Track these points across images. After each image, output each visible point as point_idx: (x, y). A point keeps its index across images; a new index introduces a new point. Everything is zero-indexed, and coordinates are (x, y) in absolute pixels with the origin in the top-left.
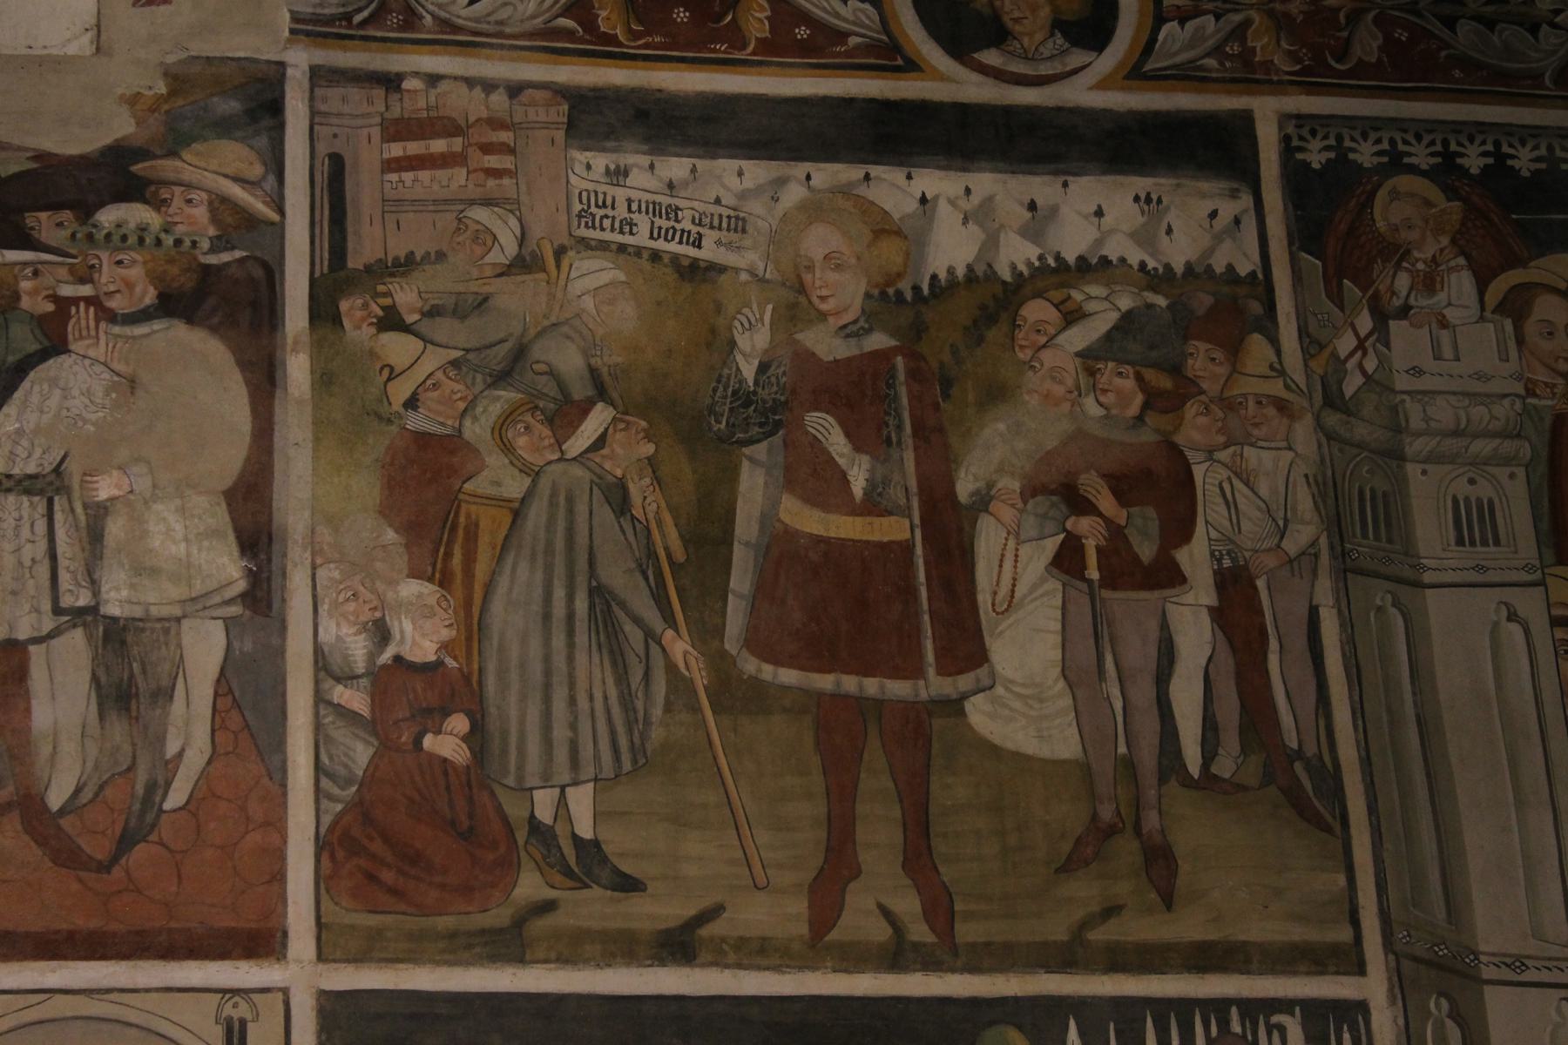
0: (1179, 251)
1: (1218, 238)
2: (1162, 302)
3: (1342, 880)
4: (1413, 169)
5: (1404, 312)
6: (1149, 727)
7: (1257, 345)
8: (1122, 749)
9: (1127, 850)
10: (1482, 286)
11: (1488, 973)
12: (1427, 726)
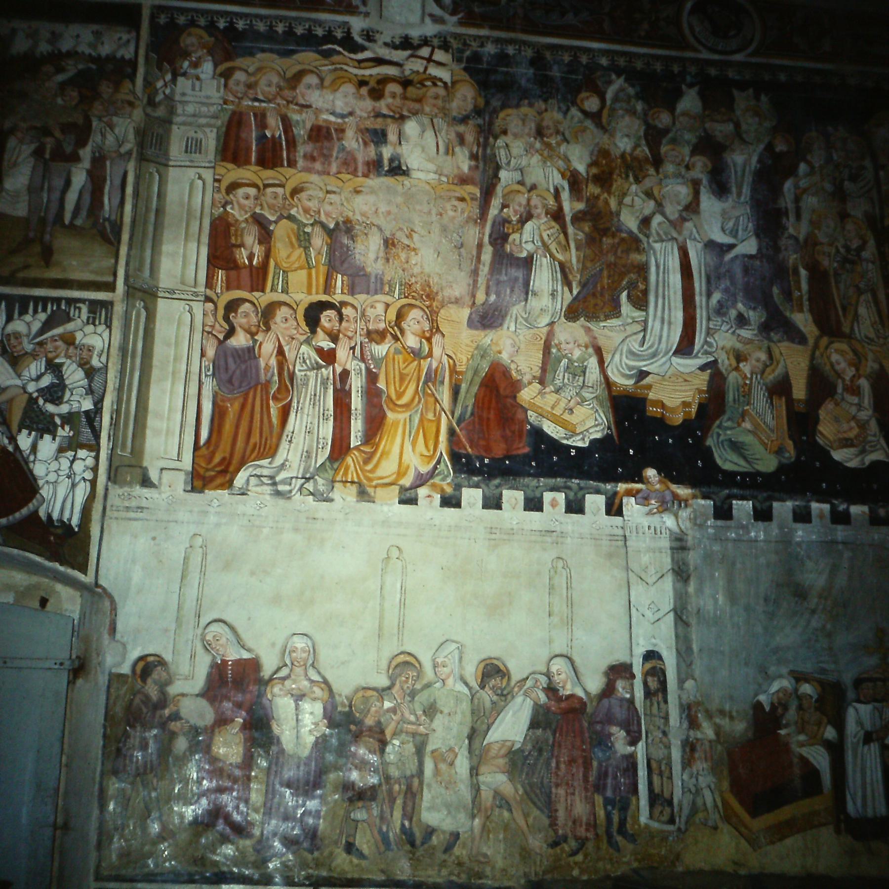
0: (105, 50)
1: (120, 47)
2: (94, 67)
3: (113, 261)
4: (199, 27)
5: (184, 74)
6: (54, 207)
7: (127, 85)
8: (42, 214)
9: (37, 249)
10: (216, 66)
11: (160, 294)
12: (160, 212)
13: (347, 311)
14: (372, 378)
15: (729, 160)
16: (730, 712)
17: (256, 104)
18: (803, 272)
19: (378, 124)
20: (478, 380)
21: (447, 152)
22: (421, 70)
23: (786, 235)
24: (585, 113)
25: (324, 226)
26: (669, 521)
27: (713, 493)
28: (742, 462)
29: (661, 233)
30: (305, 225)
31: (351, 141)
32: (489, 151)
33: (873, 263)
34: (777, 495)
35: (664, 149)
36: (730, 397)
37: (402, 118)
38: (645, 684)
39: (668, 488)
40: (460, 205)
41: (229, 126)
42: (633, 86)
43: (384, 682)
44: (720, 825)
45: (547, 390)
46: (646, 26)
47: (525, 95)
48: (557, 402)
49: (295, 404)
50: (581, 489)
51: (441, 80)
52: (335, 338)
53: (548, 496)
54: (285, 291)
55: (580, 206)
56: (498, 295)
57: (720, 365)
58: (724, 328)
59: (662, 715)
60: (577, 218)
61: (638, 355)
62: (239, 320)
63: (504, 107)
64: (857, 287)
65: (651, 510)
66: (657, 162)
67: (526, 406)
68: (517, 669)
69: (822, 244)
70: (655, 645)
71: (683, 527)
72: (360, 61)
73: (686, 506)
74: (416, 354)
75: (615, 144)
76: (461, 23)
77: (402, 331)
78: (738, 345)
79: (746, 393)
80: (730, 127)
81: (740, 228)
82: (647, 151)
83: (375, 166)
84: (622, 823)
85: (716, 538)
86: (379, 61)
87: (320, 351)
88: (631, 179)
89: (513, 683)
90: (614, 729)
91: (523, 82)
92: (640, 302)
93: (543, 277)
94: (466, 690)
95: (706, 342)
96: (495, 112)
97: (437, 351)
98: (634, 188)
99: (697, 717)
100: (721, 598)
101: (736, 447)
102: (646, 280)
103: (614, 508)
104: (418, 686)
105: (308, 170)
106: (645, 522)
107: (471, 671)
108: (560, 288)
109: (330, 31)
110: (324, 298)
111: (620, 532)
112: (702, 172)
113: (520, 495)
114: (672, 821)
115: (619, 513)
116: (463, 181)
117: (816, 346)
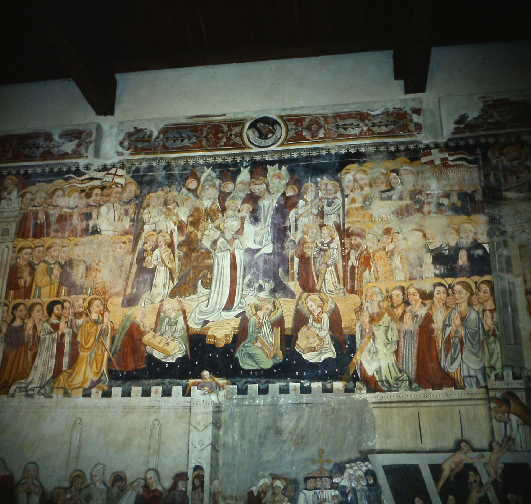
13: (66, 304)
14: (75, 335)
15: (261, 205)
16: (236, 497)
17: (34, 208)
18: (296, 260)
19: (88, 210)
20: (124, 332)
21: (119, 220)
22: (111, 180)
23: (289, 240)
24: (189, 190)
25: (60, 264)
26: (213, 397)
27: (238, 381)
30: (51, 264)
31: (76, 220)
32: (140, 216)
33: (337, 249)
34: (271, 380)
35: (227, 204)
36: (250, 330)
37: (100, 205)
39: (214, 380)
40: (123, 245)
41: (22, 221)
42: (215, 172)
43: (67, 484)
45: (157, 334)
46: (224, 140)
47: (160, 185)
48: (161, 341)
49: (39, 352)
50: (170, 383)
51: (120, 184)
52: (59, 318)
53: (153, 389)
54: (39, 297)
55: (183, 238)
56: (137, 289)
57: (246, 314)
58: (250, 294)
59: (200, 499)
60: (180, 245)
61: (205, 312)
62: (18, 313)
63: (149, 193)
64: (327, 264)
65: (205, 392)
66: (223, 210)
67: (146, 344)
68: (130, 476)
69: (308, 242)
70: (200, 462)
71: (220, 400)
72: (82, 181)
73: (223, 389)
74: (96, 322)
75: (203, 204)
76: (132, 154)
77: (90, 312)
78: (257, 302)
79: (259, 328)
80: (264, 186)
81: (264, 239)
82: (218, 205)
83: (86, 231)
86: (92, 179)
87: (52, 325)
88: (209, 221)
89: (128, 483)
91: (160, 179)
92: (207, 285)
93: (161, 277)
94: (105, 488)
95: (240, 302)
96: (145, 196)
97: (106, 320)
98: (211, 225)
99: (218, 499)
100: (236, 437)
101: (251, 356)
103: (186, 393)
104: (83, 486)
105: (55, 237)
106: (201, 398)
107: (108, 478)
108: (168, 282)
109: (69, 168)
110: (56, 299)
111: (188, 405)
112: (246, 213)
113: (140, 389)
115: (189, 395)
116: (126, 233)
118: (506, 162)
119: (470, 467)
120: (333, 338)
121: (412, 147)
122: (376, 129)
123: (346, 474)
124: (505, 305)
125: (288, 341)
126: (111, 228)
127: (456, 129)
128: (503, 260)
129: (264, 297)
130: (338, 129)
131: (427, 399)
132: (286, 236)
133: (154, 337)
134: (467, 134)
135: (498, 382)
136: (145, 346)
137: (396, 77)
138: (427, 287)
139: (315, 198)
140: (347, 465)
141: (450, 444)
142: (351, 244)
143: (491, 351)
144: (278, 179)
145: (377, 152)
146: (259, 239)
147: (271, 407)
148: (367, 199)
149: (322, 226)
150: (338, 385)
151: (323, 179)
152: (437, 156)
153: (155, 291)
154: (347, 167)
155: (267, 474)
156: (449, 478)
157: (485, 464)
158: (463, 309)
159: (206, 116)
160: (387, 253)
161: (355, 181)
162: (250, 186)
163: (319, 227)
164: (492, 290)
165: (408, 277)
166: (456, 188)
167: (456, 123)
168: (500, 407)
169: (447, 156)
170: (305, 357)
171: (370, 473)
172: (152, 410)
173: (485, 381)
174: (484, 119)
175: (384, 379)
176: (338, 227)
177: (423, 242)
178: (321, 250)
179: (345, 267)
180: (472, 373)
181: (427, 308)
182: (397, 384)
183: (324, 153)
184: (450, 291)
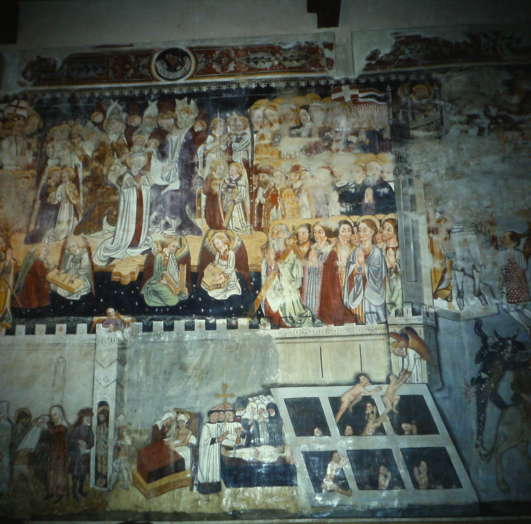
15: (169, 140)
16: (141, 431)
18: (204, 197)
20: (28, 270)
21: (21, 154)
22: (13, 112)
23: (197, 176)
24: (95, 124)
26: (119, 335)
27: (143, 318)
28: (159, 301)
29: (128, 183)
32: (43, 150)
33: (245, 186)
34: (177, 317)
35: (134, 138)
36: (156, 267)
38: (98, 418)
39: (119, 318)
40: (26, 180)
42: (122, 105)
44: (130, 487)
45: (61, 272)
46: (132, 71)
47: (65, 118)
50: (75, 321)
51: (22, 116)
53: (58, 326)
55: (87, 174)
56: (41, 226)
57: (152, 251)
58: (157, 230)
59: (105, 433)
60: (85, 180)
61: (110, 250)
63: (53, 126)
64: (234, 201)
65: (110, 329)
66: (130, 145)
67: (50, 281)
68: (35, 413)
69: (216, 179)
70: (105, 398)
71: (125, 337)
73: (128, 326)
75: (109, 139)
76: (35, 85)
78: (164, 239)
79: (165, 265)
80: (172, 120)
81: (171, 176)
82: (125, 139)
84: (81, 487)
85: (144, 342)
88: (115, 156)
89: (32, 420)
90: (80, 441)
91: (64, 112)
92: (113, 222)
93: (65, 214)
94: (9, 424)
95: (146, 239)
96: (48, 129)
97: (9, 257)
98: (116, 160)
99: (123, 434)
100: (141, 373)
101: (156, 293)
102: (117, 209)
103: (92, 330)
106: (106, 336)
107: (12, 415)
108: (72, 218)
111: (93, 342)
112: (154, 148)
113: (44, 327)
114: (106, 486)
115: (94, 332)
117: (207, 235)
118: (416, 101)
119: (368, 399)
120: (238, 275)
121: (322, 83)
122: (287, 64)
123: (249, 407)
124: (407, 243)
125: (194, 278)
126: (14, 162)
127: (367, 65)
128: (408, 198)
129: (170, 234)
130: (248, 62)
131: (329, 335)
132: (193, 172)
133: (58, 274)
134: (379, 71)
135: (398, 317)
136: (49, 283)
137: (310, 10)
138: (333, 225)
139: (224, 134)
140: (250, 399)
141: (349, 377)
142: (259, 181)
143: (392, 288)
144: (186, 114)
145: (288, 87)
146: (166, 175)
147: (176, 344)
148: (276, 135)
149: (230, 162)
150: (243, 321)
151: (232, 115)
152: (347, 93)
153: (59, 227)
154: (257, 103)
155: (171, 408)
156: (347, 410)
157: (382, 396)
158: (367, 246)
159: (113, 46)
160: (294, 191)
161: (265, 117)
162: (157, 120)
163: (227, 164)
164: (396, 228)
165: (314, 214)
166: (365, 126)
167: (368, 59)
168: (398, 342)
169: (357, 93)
170: (211, 294)
171: (272, 406)
172: (57, 348)
173: (386, 316)
174: (395, 55)
175: (288, 315)
176: (246, 164)
177: (330, 179)
178: (229, 187)
179: (252, 204)
180: (373, 309)
181: (331, 246)
182: (301, 320)
183: (234, 87)
184: (355, 229)
